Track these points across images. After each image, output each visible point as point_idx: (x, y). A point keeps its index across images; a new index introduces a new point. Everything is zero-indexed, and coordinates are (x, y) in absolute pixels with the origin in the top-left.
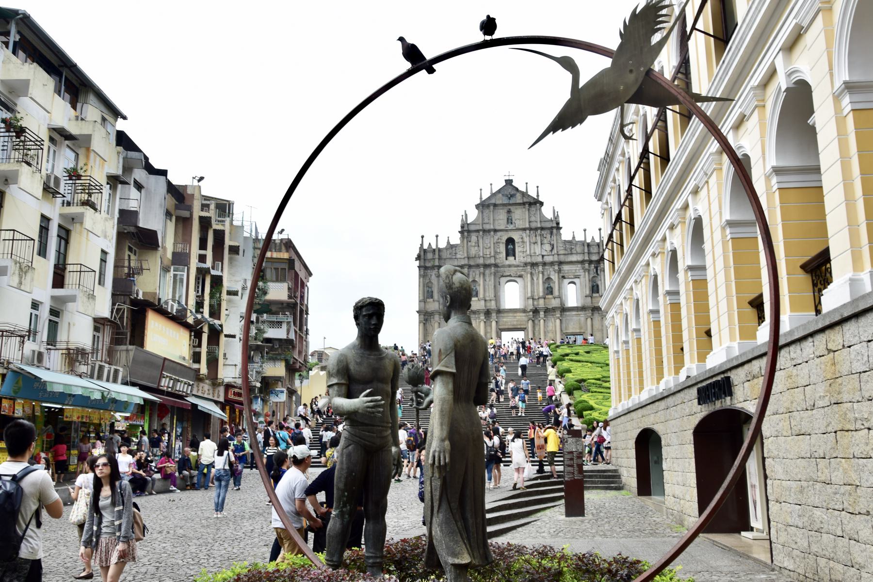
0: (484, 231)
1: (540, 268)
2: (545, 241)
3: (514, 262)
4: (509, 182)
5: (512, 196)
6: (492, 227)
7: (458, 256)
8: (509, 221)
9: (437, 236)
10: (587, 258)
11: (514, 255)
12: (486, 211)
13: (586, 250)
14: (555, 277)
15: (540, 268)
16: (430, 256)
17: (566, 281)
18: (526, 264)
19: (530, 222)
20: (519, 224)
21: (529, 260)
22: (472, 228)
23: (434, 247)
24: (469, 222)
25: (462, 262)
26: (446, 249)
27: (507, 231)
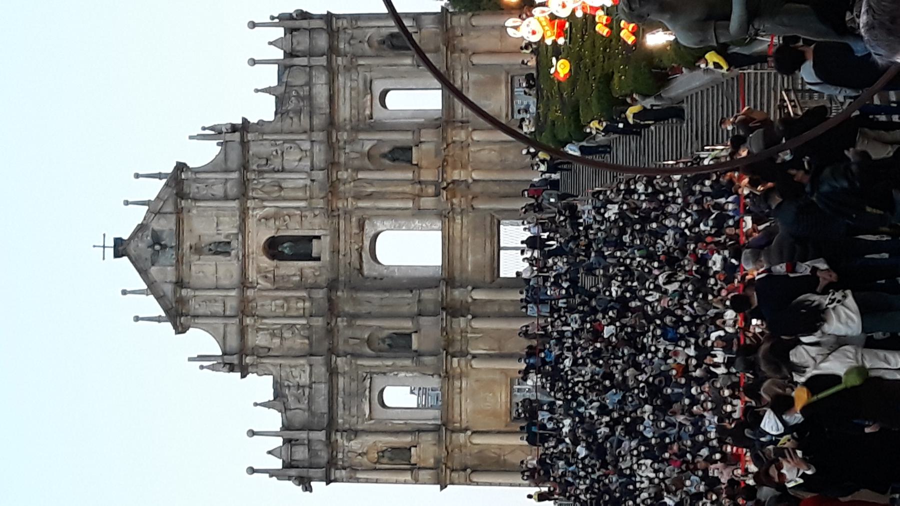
1: (344, 175)
2: (276, 163)
3: (326, 241)
4: (120, 248)
5: (157, 239)
7: (305, 379)
8: (221, 249)
9: (252, 433)
10: (323, 61)
11: (310, 239)
12: (195, 306)
13: (303, 61)
14: (367, 141)
15: (344, 175)
16: (301, 453)
17: (379, 114)
19: (226, 198)
20: (229, 227)
21: (321, 203)
22: (233, 342)
23: (278, 442)
24: (221, 353)
25: (321, 370)
26: (285, 410)
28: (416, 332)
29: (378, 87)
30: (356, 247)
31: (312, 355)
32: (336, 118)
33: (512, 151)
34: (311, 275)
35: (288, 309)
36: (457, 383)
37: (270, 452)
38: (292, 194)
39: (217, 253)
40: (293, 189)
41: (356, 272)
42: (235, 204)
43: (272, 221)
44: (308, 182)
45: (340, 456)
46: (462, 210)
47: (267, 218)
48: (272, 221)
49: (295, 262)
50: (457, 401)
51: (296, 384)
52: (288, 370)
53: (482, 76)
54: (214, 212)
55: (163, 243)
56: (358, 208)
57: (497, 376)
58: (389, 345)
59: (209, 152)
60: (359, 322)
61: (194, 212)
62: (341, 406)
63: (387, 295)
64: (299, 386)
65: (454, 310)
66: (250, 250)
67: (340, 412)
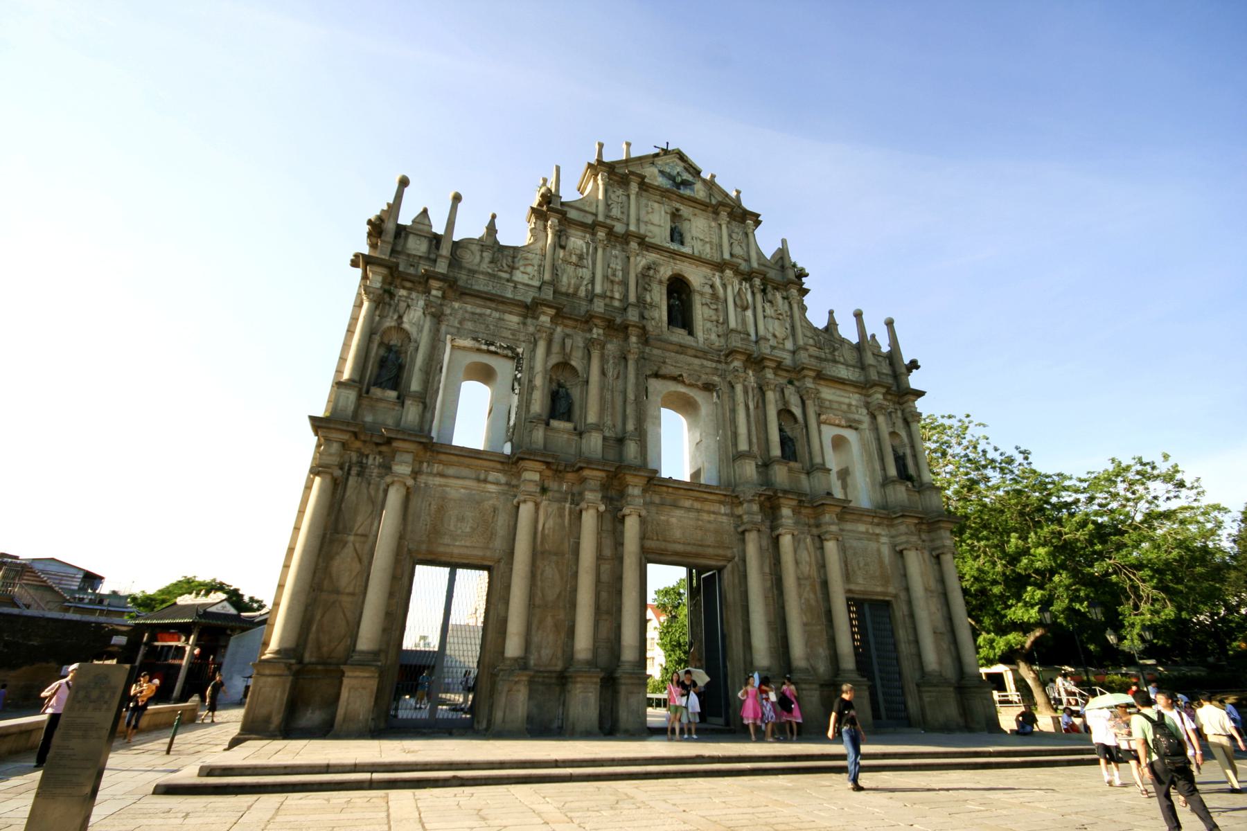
0: (610, 232)
1: (769, 374)
7: (518, 276)
8: (677, 235)
9: (457, 198)
16: (417, 246)
19: (732, 255)
22: (573, 214)
23: (439, 228)
28: (575, 429)
29: (849, 434)
33: (812, 596)
35: (612, 282)
36: (493, 476)
37: (425, 211)
39: (673, 231)
40: (744, 322)
42: (727, 256)
44: (753, 337)
45: (403, 292)
47: (712, 286)
50: (465, 472)
52: (536, 262)
53: (887, 560)
57: (499, 544)
58: (557, 392)
59: (768, 253)
61: (713, 224)
62: (478, 310)
64: (513, 268)
67: (469, 307)
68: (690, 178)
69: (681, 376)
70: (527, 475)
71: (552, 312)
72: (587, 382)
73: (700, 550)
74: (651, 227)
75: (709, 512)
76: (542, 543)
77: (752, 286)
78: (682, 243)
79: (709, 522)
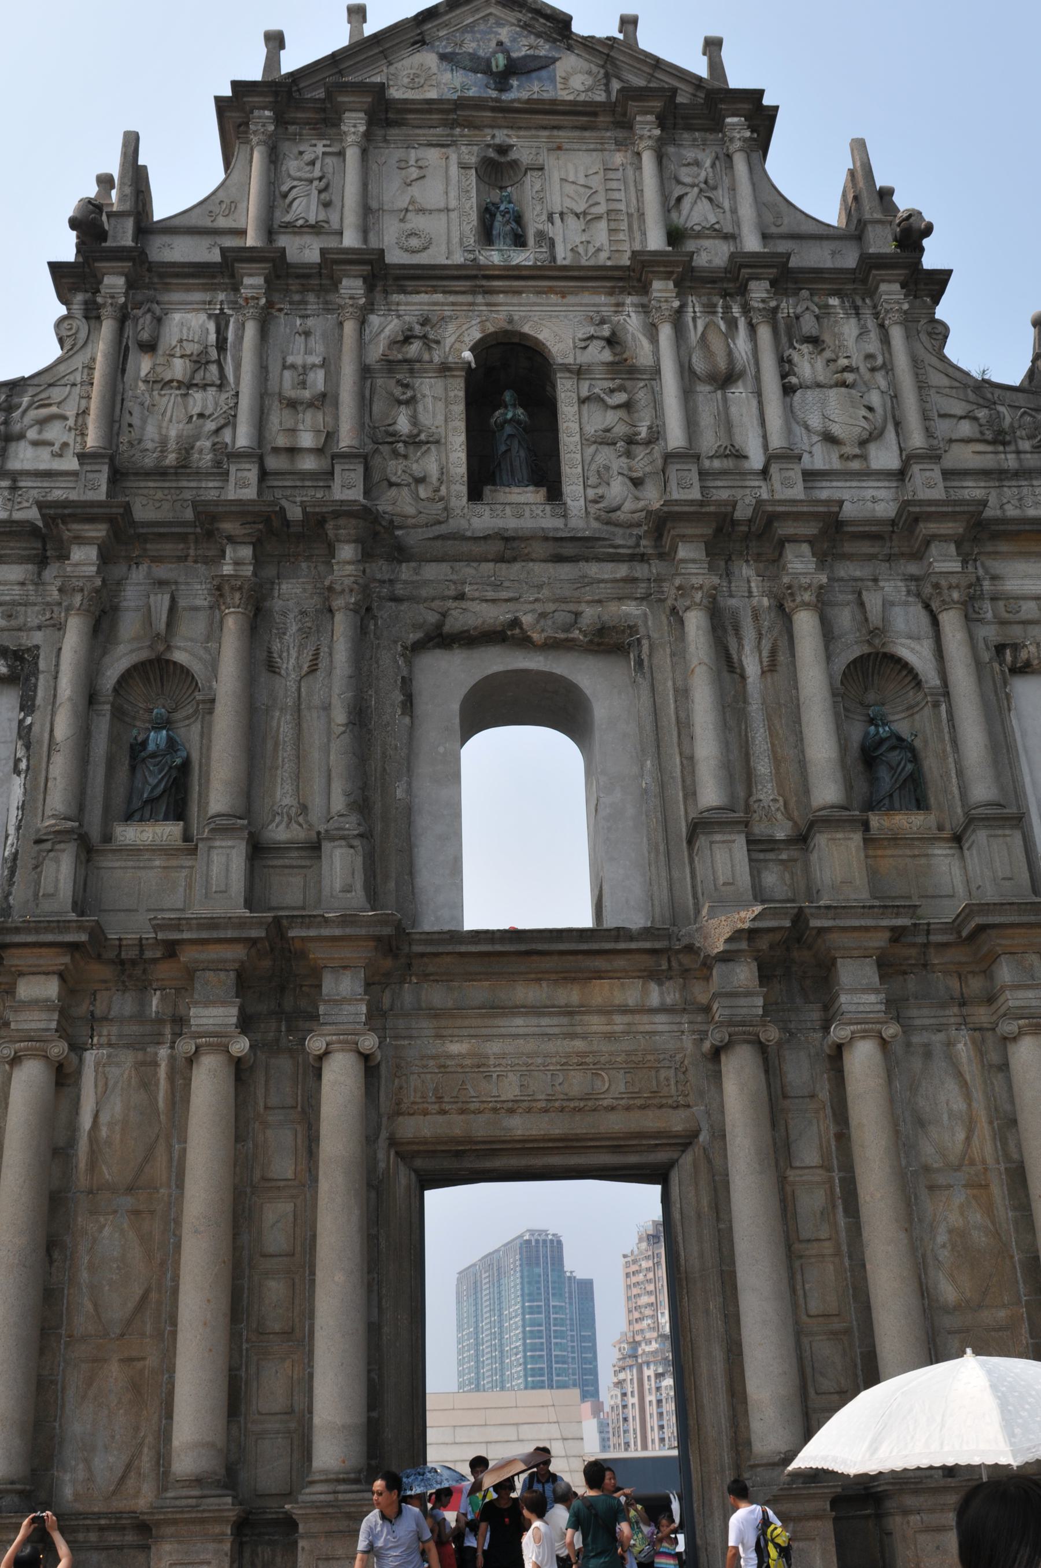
1: (800, 563)
2: (808, 366)
6: (350, 240)
7: (24, 457)
11: (547, 477)
15: (800, 563)
18: (662, 524)
21: (686, 489)
27: (473, 279)
28: (187, 837)
30: (527, 620)
31: (117, 476)
32: (1004, 547)
33: (977, 1217)
34: (416, 469)
35: (293, 404)
38: (706, 419)
39: (487, 215)
40: (726, 424)
41: (432, 618)
42: (656, 241)
43: (607, 356)
44: (756, 460)
46: (707, 1009)
48: (607, 356)
49: (461, 425)
51: (17, 428)
54: (622, 206)
55: (515, 83)
56: (676, 617)
58: (144, 744)
60: (232, 624)
61: (619, 158)
63: (340, 716)
65: (275, 981)
66: (501, 298)
68: (544, 49)
69: (515, 623)
70: (28, 989)
71: (99, 531)
72: (213, 701)
73: (580, 1126)
74: (417, 222)
75: (607, 1011)
76: (93, 1164)
77: (746, 309)
78: (519, 241)
79: (609, 1036)
